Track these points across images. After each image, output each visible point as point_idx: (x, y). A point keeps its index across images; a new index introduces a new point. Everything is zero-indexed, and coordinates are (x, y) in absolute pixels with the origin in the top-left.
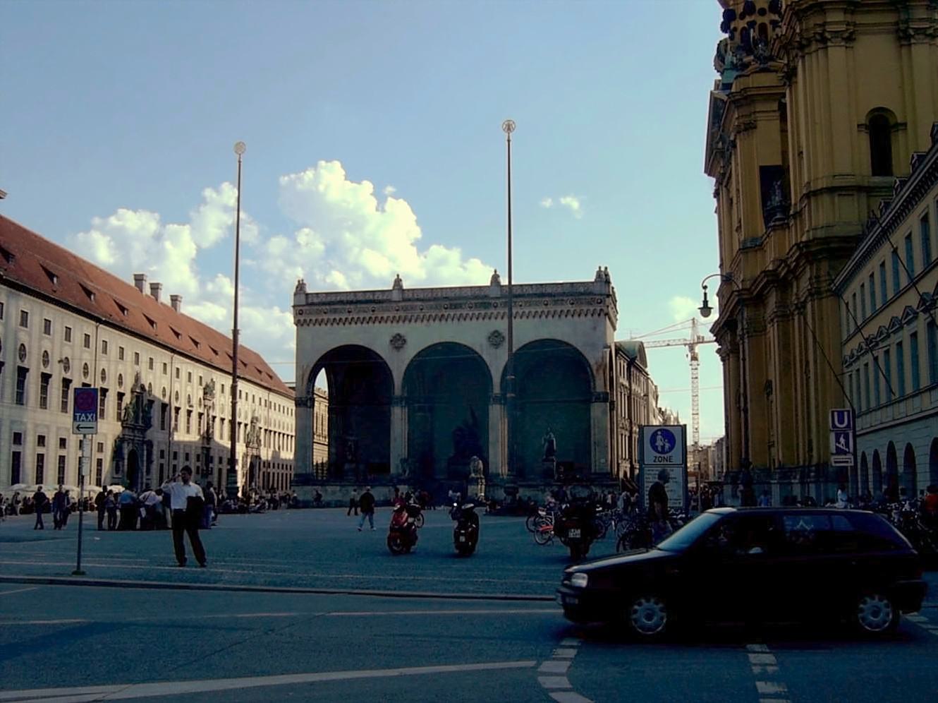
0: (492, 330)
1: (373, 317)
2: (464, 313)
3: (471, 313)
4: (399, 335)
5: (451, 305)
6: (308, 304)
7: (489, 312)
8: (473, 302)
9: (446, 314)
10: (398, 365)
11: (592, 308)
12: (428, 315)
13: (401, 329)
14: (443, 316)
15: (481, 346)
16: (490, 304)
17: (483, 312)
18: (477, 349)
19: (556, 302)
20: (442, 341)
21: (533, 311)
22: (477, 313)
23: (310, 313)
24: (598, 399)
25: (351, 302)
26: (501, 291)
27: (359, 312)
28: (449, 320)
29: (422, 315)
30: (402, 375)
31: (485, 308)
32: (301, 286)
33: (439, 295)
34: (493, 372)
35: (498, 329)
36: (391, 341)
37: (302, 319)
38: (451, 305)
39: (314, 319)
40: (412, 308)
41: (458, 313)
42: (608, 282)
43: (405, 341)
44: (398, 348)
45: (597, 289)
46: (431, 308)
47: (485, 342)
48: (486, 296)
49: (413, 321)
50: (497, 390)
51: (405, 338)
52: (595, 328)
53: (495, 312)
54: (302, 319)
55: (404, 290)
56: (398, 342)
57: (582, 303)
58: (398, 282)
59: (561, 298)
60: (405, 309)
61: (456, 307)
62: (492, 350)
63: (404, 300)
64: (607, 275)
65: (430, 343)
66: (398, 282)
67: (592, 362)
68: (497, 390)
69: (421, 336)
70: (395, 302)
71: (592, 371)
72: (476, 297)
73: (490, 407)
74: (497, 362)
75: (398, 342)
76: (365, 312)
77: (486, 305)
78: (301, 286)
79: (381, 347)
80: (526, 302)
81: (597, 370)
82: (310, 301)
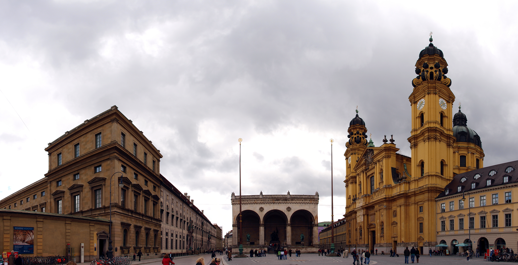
0: (288, 207)
1: (254, 202)
3: (282, 202)
4: (262, 207)
5: (277, 200)
7: (287, 202)
8: (283, 199)
9: (275, 202)
10: (262, 215)
11: (314, 202)
12: (270, 202)
15: (285, 211)
16: (287, 200)
17: (285, 202)
18: (284, 212)
19: (305, 200)
20: (274, 209)
22: (284, 202)
26: (290, 196)
28: (276, 204)
29: (268, 202)
30: (263, 218)
31: (286, 201)
33: (273, 197)
36: (260, 209)
38: (277, 200)
41: (279, 202)
43: (263, 209)
44: (262, 211)
47: (286, 210)
48: (286, 198)
49: (266, 204)
51: (264, 208)
53: (289, 202)
56: (262, 209)
59: (306, 199)
61: (278, 200)
62: (288, 212)
65: (271, 210)
68: (289, 222)
69: (268, 208)
71: (314, 219)
72: (284, 198)
74: (289, 215)
75: (262, 209)
77: (286, 200)
80: (297, 200)
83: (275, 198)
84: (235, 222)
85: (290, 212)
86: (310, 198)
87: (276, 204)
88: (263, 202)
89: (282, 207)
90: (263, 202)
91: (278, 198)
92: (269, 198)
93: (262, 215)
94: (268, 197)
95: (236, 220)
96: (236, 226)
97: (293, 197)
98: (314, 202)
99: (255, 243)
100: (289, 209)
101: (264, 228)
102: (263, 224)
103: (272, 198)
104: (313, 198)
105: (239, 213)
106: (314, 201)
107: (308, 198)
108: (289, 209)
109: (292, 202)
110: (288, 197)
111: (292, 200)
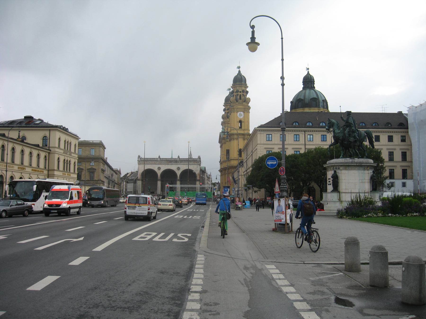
2: (172, 163)
6: (141, 160)
7: (177, 163)
10: (159, 173)
12: (165, 163)
13: (160, 166)
14: (168, 164)
17: (176, 163)
18: (175, 170)
21: (186, 164)
22: (175, 163)
23: (141, 162)
24: (198, 181)
25: (150, 161)
27: (151, 162)
28: (169, 165)
30: (160, 175)
32: (139, 156)
34: (178, 175)
35: (179, 166)
37: (140, 163)
39: (142, 163)
40: (162, 162)
41: (171, 163)
42: (200, 159)
43: (160, 168)
44: (159, 170)
45: (198, 160)
46: (166, 162)
47: (176, 169)
48: (177, 160)
50: (178, 178)
52: (197, 167)
53: (178, 163)
54: (140, 163)
55: (160, 158)
56: (159, 168)
57: (195, 162)
58: (159, 157)
60: (161, 162)
61: (171, 162)
62: (178, 171)
63: (160, 160)
64: (200, 157)
66: (159, 157)
67: (197, 174)
68: (178, 178)
69: (164, 167)
70: (159, 161)
72: (175, 160)
73: (177, 182)
74: (179, 173)
75: (159, 168)
76: (153, 162)
77: (177, 162)
78: (139, 156)
79: (156, 169)
81: (198, 175)
82: (141, 159)
83: (169, 161)
84: (140, 177)
85: (179, 171)
86: (193, 161)
87: (169, 165)
88: (160, 163)
89: (173, 167)
90: (160, 163)
91: (171, 160)
92: (165, 160)
93: (159, 173)
94: (164, 160)
95: (141, 175)
96: (141, 180)
97: (181, 160)
98: (197, 164)
99: (155, 192)
100: (179, 169)
101: (160, 182)
102: (160, 179)
103: (167, 160)
104: (196, 161)
105: (144, 170)
106: (196, 163)
107: (192, 161)
108: (179, 169)
109: (181, 163)
110: (178, 160)
111: (181, 162)
